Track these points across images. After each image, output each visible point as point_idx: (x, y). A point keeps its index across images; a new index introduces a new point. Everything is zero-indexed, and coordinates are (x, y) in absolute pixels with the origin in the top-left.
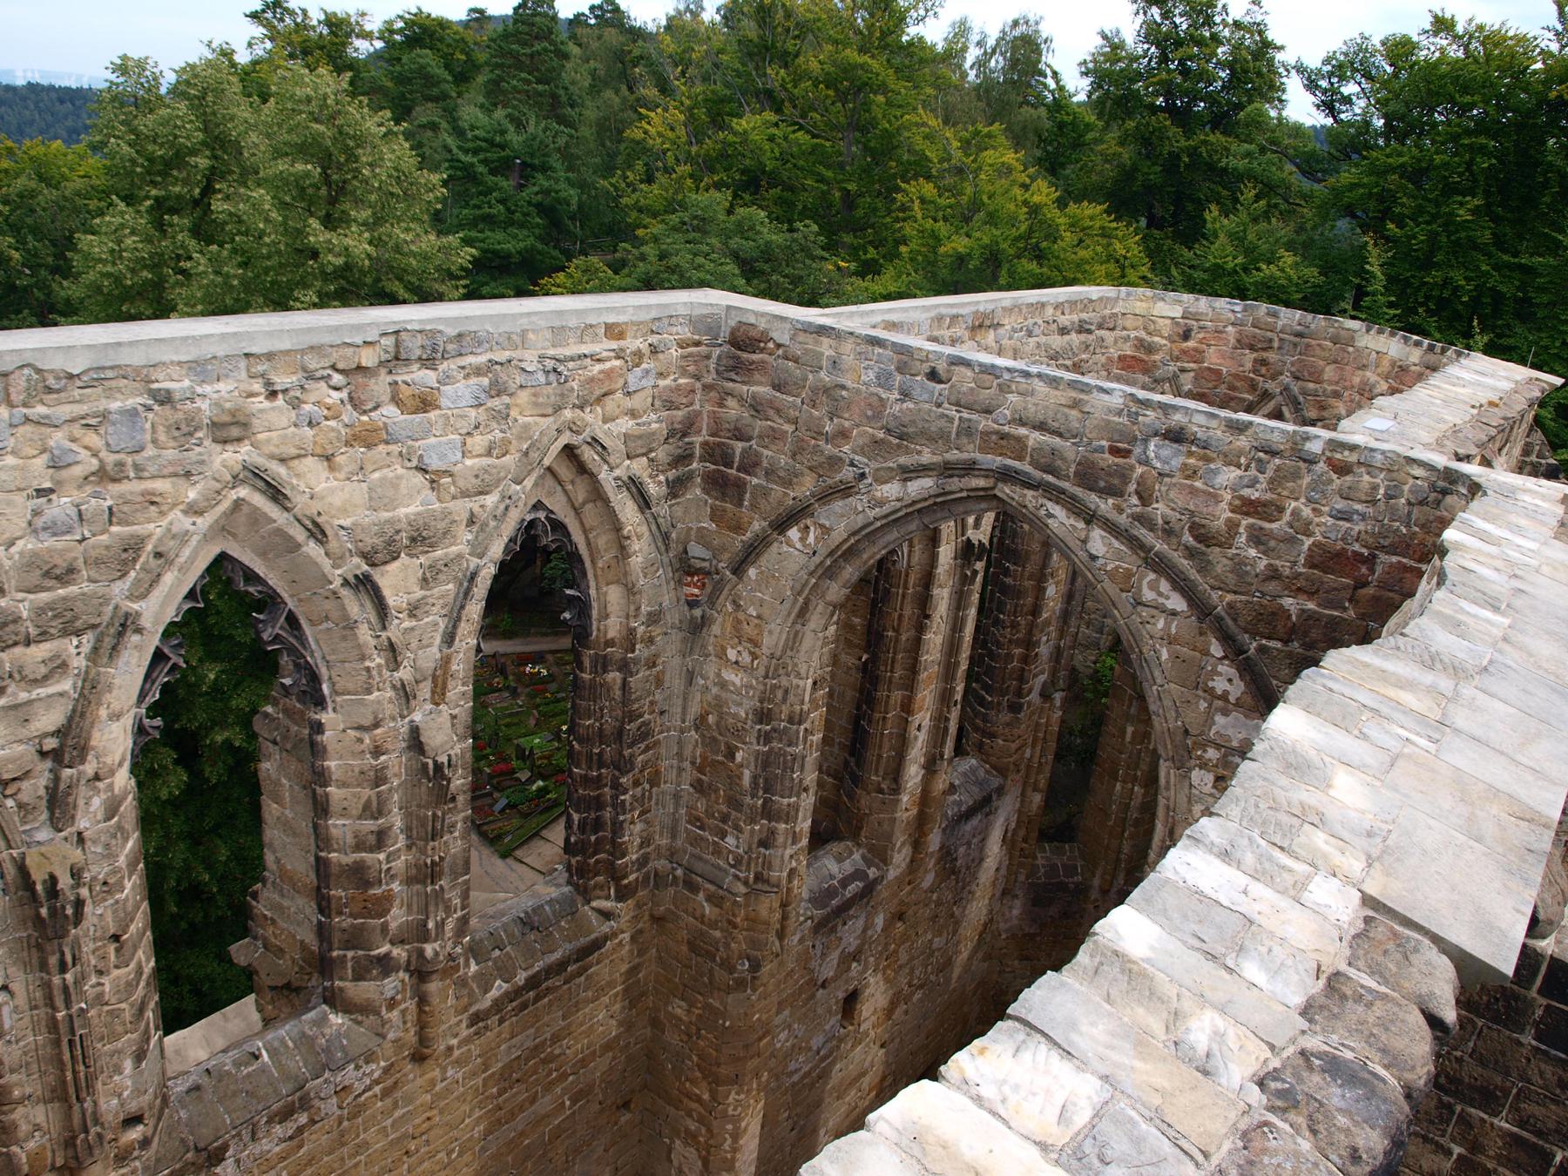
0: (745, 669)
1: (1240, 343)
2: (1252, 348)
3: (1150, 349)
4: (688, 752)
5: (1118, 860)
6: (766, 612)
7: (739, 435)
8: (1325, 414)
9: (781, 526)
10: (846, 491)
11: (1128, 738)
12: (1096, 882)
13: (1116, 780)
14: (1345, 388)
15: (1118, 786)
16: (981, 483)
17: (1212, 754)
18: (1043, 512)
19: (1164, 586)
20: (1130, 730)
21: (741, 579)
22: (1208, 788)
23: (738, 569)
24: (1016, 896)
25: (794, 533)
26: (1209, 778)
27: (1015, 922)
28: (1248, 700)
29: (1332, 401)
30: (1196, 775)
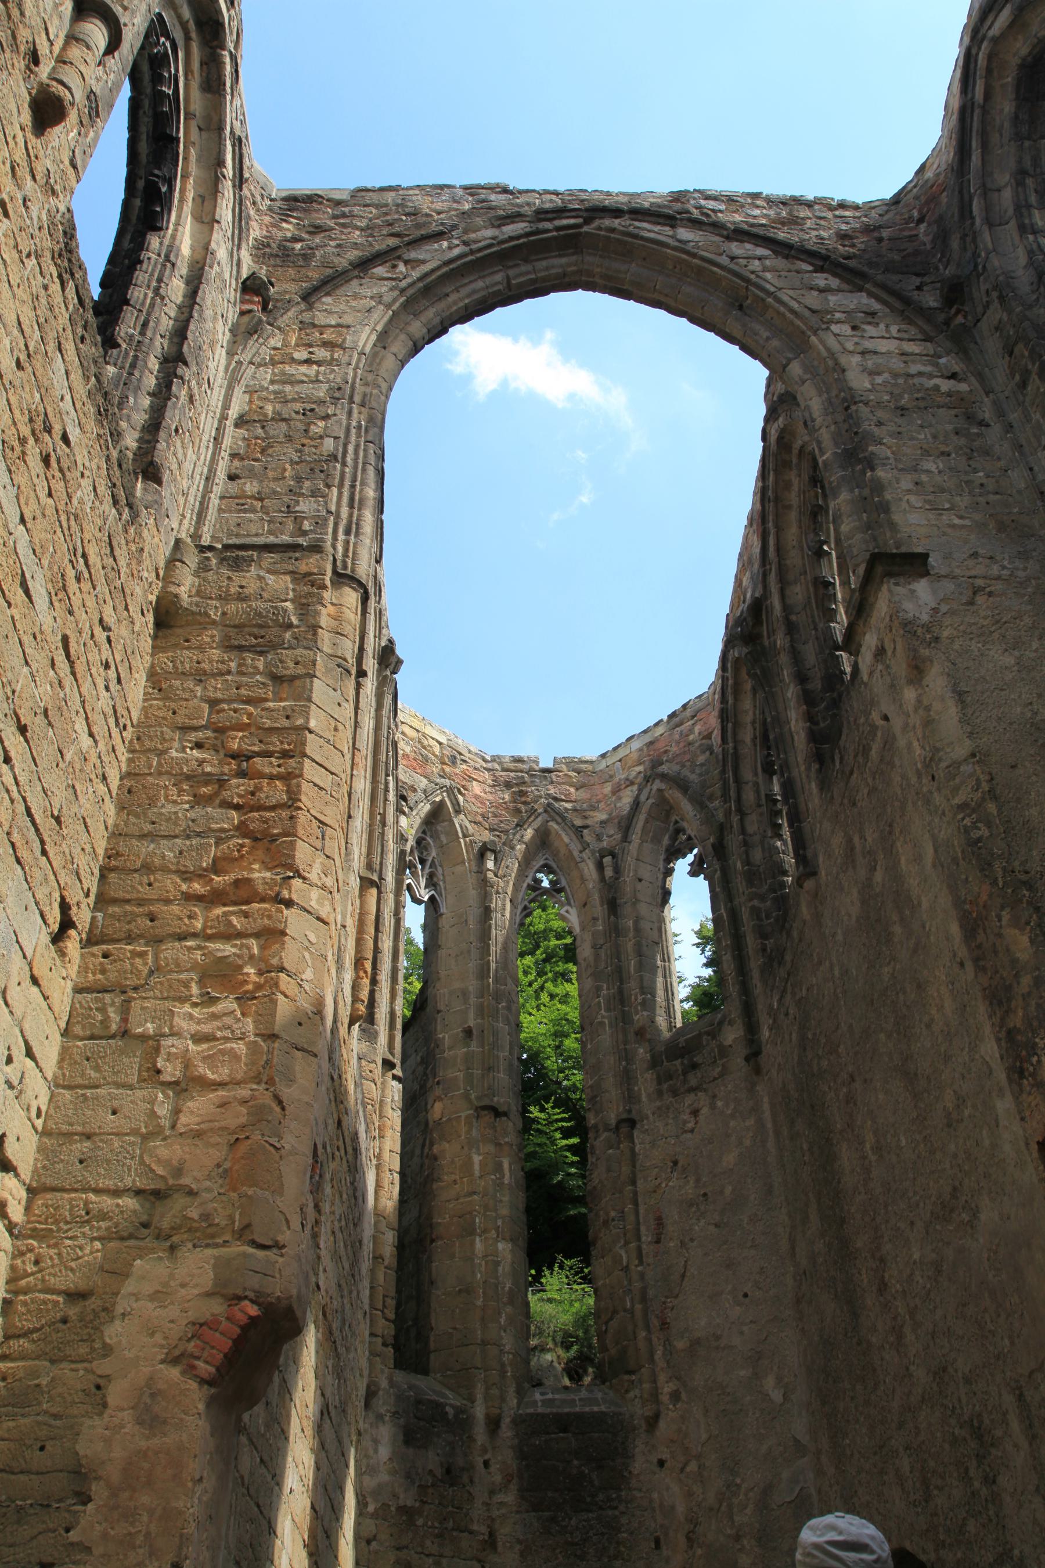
0: (319, 363)
1: (496, 783)
2: (508, 785)
3: (426, 759)
4: (227, 442)
5: (503, 1365)
6: (347, 319)
7: (296, 239)
8: (589, 822)
9: (364, 265)
10: (439, 236)
11: (477, 1173)
12: (479, 1411)
13: (470, 1231)
14: (599, 802)
15: (479, 1245)
16: (572, 221)
17: (838, 315)
18: (631, 229)
19: (748, 246)
20: (477, 1159)
21: (310, 307)
22: (849, 332)
23: (308, 297)
24: (380, 1417)
25: (380, 271)
26: (846, 329)
27: (384, 1477)
28: (845, 286)
29: (591, 813)
30: (834, 328)
